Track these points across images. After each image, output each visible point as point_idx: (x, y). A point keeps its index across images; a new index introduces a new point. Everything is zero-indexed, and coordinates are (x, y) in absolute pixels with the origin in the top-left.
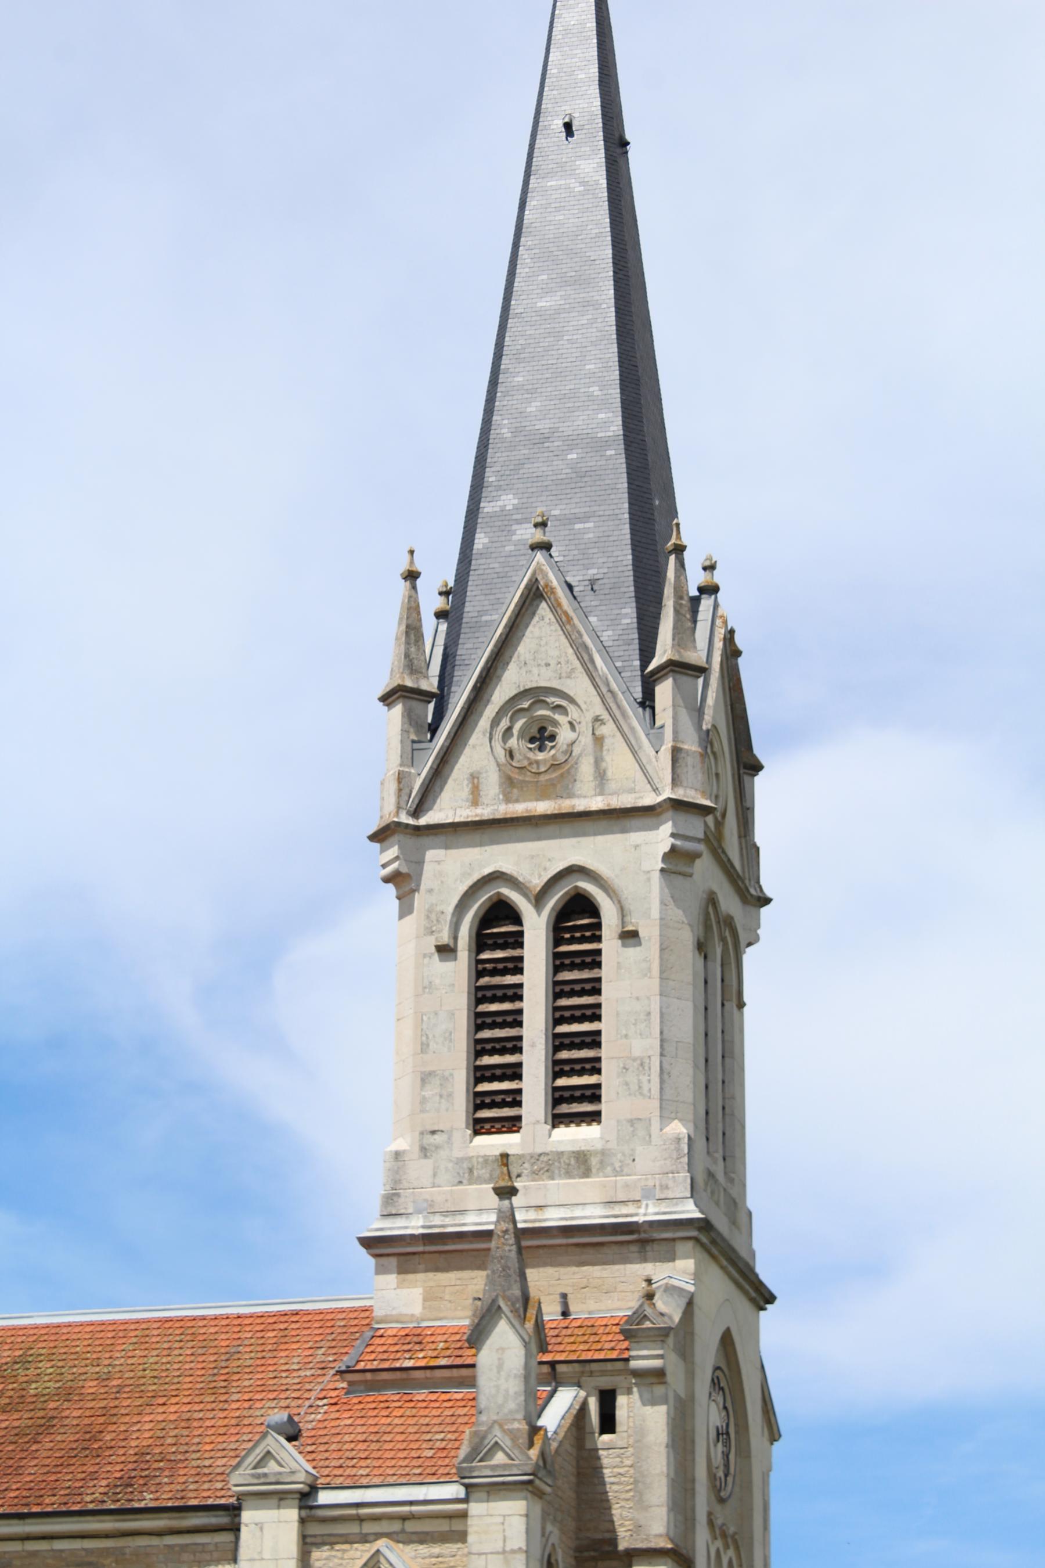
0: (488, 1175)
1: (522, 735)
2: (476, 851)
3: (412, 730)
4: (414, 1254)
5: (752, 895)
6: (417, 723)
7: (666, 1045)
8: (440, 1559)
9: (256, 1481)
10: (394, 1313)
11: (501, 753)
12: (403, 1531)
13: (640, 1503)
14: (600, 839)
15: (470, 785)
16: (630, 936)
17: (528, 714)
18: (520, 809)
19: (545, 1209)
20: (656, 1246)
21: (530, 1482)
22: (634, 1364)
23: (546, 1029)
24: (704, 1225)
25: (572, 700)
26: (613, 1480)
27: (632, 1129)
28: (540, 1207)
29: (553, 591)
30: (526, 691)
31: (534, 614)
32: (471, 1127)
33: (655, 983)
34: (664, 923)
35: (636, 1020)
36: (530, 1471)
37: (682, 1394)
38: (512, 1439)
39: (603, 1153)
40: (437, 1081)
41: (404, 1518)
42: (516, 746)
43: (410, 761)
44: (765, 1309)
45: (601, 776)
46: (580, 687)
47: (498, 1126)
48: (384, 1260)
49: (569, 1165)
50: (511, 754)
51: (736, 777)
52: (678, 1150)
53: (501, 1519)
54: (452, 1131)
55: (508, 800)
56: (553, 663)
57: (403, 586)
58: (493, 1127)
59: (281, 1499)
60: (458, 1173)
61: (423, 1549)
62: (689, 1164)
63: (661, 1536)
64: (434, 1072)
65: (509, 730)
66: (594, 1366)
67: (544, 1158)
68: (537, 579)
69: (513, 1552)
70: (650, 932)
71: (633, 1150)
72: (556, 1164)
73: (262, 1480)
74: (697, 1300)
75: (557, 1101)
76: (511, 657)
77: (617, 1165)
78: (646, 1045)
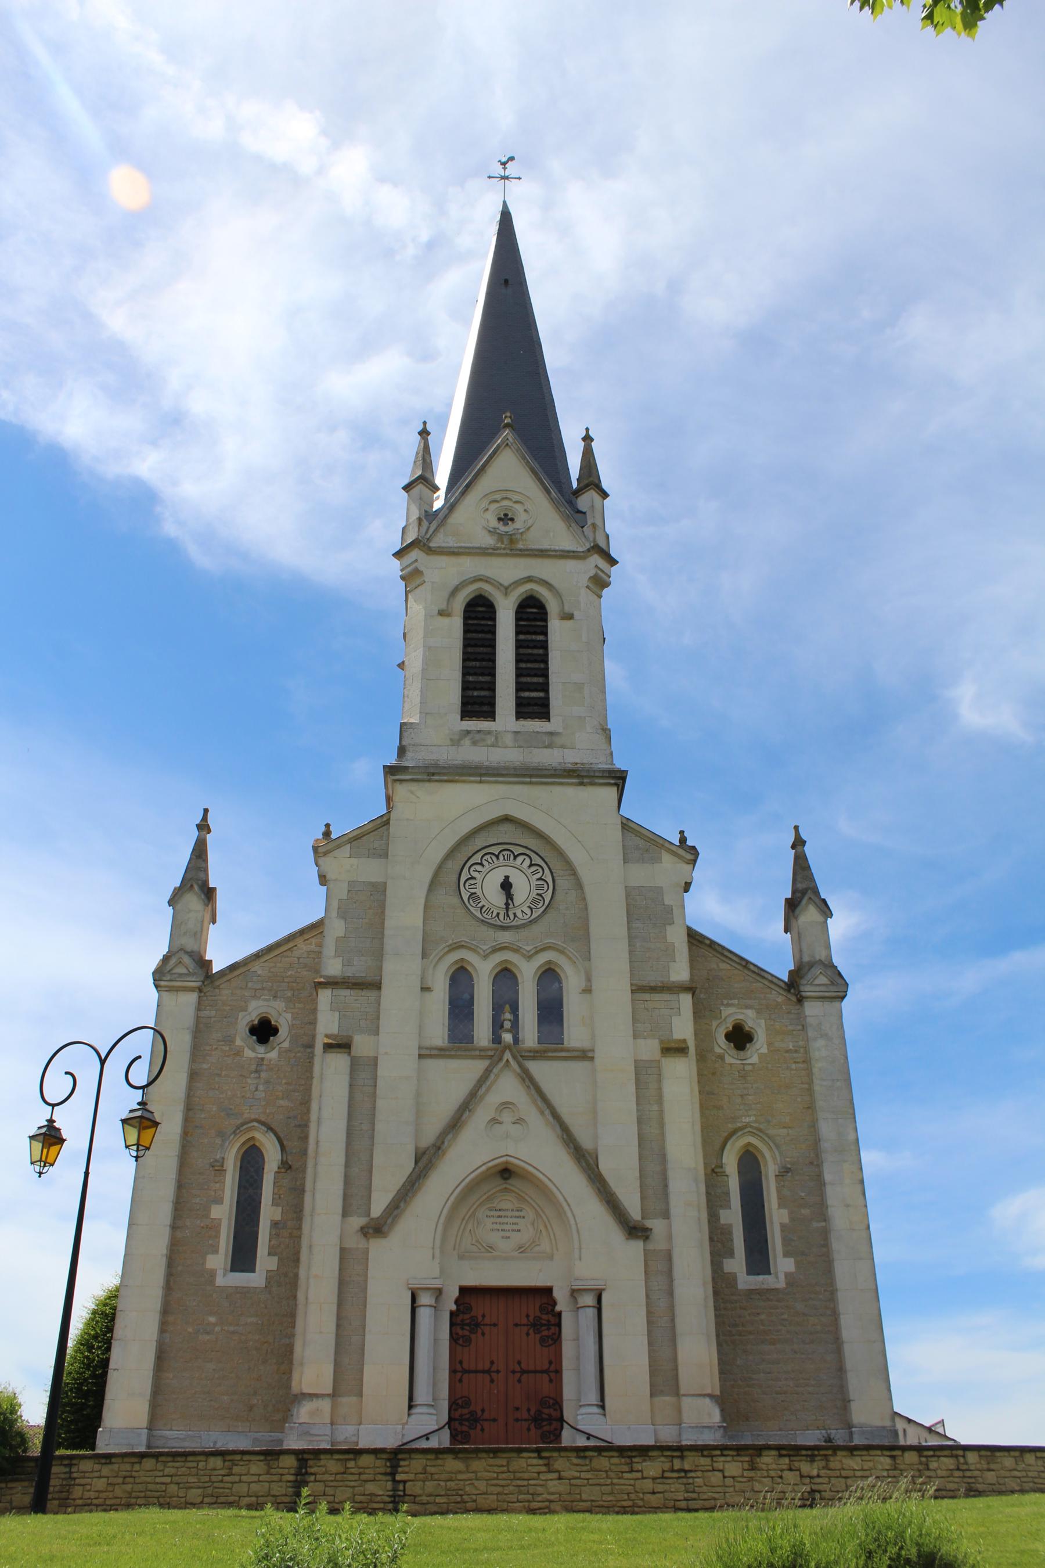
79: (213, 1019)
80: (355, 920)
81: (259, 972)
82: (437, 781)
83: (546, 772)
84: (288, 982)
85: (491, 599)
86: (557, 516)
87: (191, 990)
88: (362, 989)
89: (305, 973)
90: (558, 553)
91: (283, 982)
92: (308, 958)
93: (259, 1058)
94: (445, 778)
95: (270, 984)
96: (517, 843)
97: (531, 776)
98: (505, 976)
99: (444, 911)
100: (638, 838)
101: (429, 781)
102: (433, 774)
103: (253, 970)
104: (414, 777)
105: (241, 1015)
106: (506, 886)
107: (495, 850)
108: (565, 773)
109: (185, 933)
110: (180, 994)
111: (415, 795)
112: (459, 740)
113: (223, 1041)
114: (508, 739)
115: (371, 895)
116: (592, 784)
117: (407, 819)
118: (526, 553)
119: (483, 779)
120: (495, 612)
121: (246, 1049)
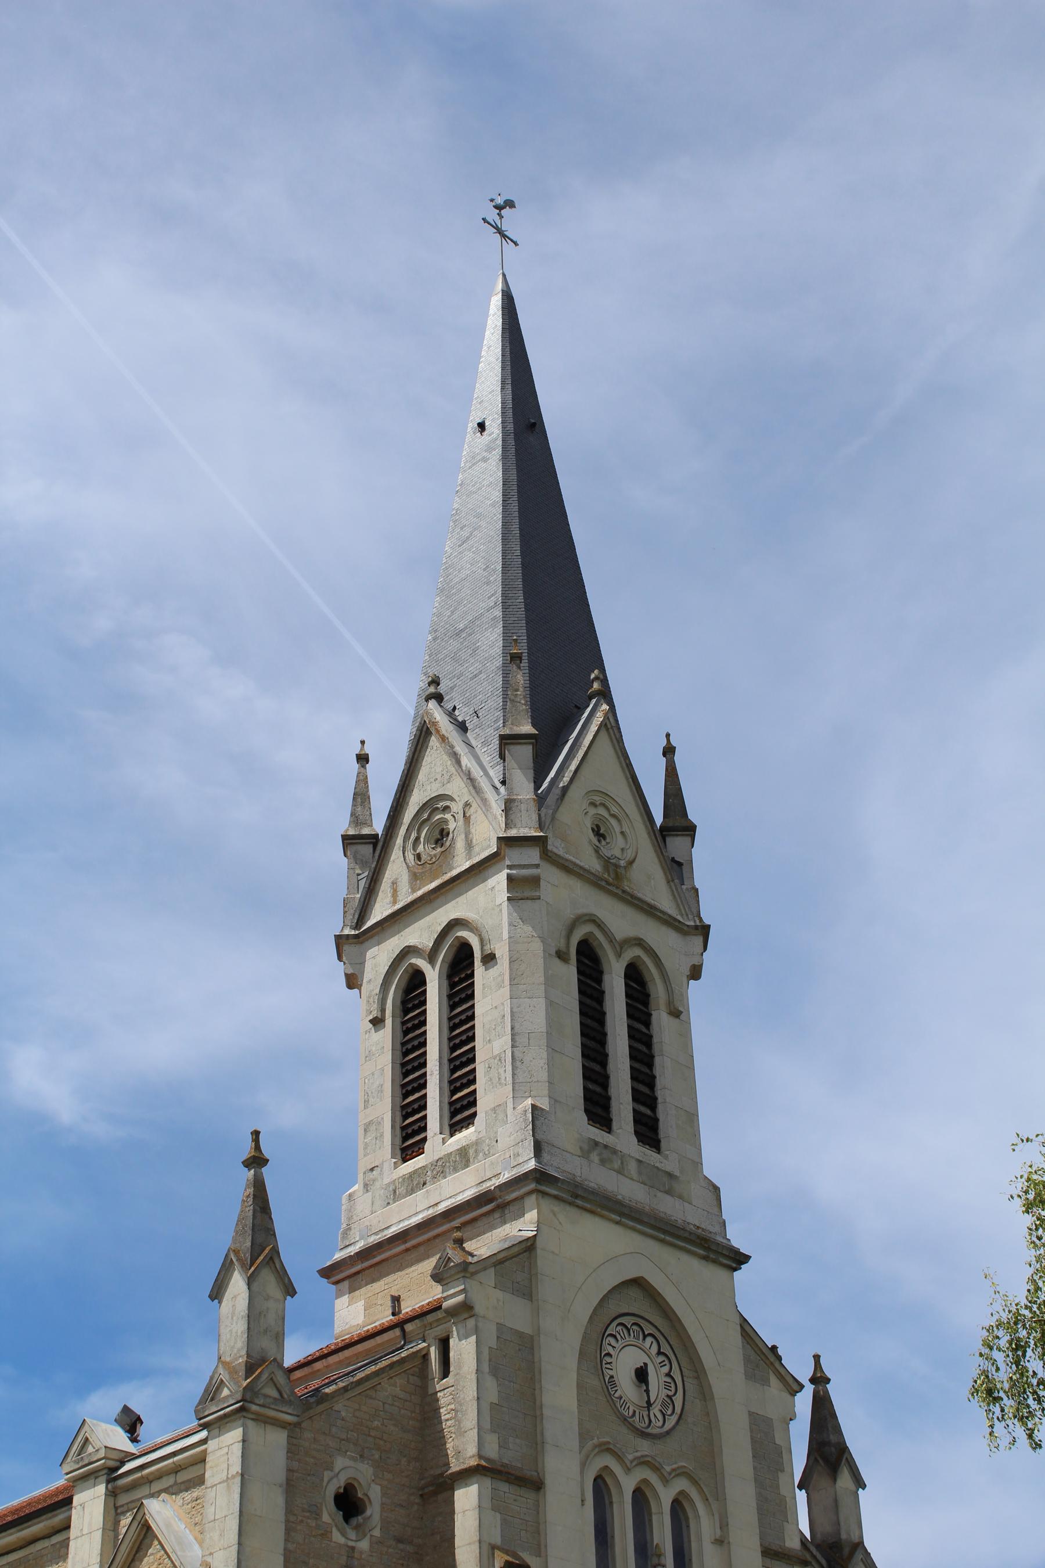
0: (405, 1191)
1: (427, 840)
2: (396, 937)
3: (357, 867)
4: (358, 1273)
5: (688, 926)
6: (362, 860)
7: (517, 1038)
8: (198, 1501)
9: (77, 1466)
10: (347, 1327)
11: (410, 857)
12: (176, 1483)
13: (461, 1433)
14: (470, 893)
15: (392, 891)
16: (489, 959)
17: (429, 823)
18: (420, 893)
19: (439, 1205)
20: (511, 1208)
21: (242, 1409)
22: (445, 1305)
23: (440, 1058)
24: (539, 1176)
25: (452, 799)
26: (447, 1416)
27: (495, 1115)
28: (436, 1204)
29: (435, 724)
30: (424, 805)
31: (427, 747)
32: (399, 1156)
33: (506, 991)
34: (512, 940)
35: (495, 1025)
36: (240, 1398)
37: (528, 1330)
38: (230, 1373)
39: (477, 1143)
40: (373, 1128)
41: (177, 1469)
42: (423, 850)
43: (357, 890)
44: (741, 1268)
45: (469, 845)
46: (458, 789)
47: (416, 1149)
48: (340, 1285)
49: (456, 1161)
50: (418, 857)
51: (652, 834)
52: (525, 1120)
53: (226, 1450)
54: (383, 1164)
55: (414, 891)
56: (439, 776)
57: (356, 766)
58: (413, 1152)
59: (96, 1478)
60: (387, 1196)
61: (188, 1496)
62: (533, 1130)
63: (473, 1456)
64: (372, 1120)
65: (417, 839)
66: (430, 1318)
67: (440, 1163)
68: (425, 721)
69: (233, 1477)
70: (502, 951)
71: (496, 1133)
72: (448, 1164)
73: (81, 1464)
74: (539, 1243)
75: (453, 1114)
76: (414, 786)
77: (486, 1149)
78: (502, 1044)
79: (295, 1474)
80: (507, 1382)
81: (343, 1414)
82: (578, 1206)
83: (681, 1233)
84: (375, 1438)
85: (600, 953)
86: (656, 860)
87: (282, 1425)
88: (520, 1486)
89: (392, 1428)
90: (665, 917)
91: (369, 1436)
92: (393, 1405)
93: (348, 1546)
94: (588, 1206)
95: (355, 1435)
96: (647, 1317)
97: (665, 1232)
98: (641, 1498)
99: (587, 1394)
100: (749, 1346)
101: (571, 1204)
102: (577, 1196)
103: (336, 1408)
104: (560, 1194)
105: (327, 1475)
106: (641, 1375)
107: (627, 1321)
108: (698, 1241)
109: (266, 1331)
110: (269, 1427)
111: (558, 1219)
112: (589, 1151)
113: (309, 1511)
114: (632, 1167)
115: (519, 1350)
116: (715, 1261)
117: (553, 1252)
118: (636, 902)
119: (623, 1220)
120: (601, 973)
121: (334, 1530)
